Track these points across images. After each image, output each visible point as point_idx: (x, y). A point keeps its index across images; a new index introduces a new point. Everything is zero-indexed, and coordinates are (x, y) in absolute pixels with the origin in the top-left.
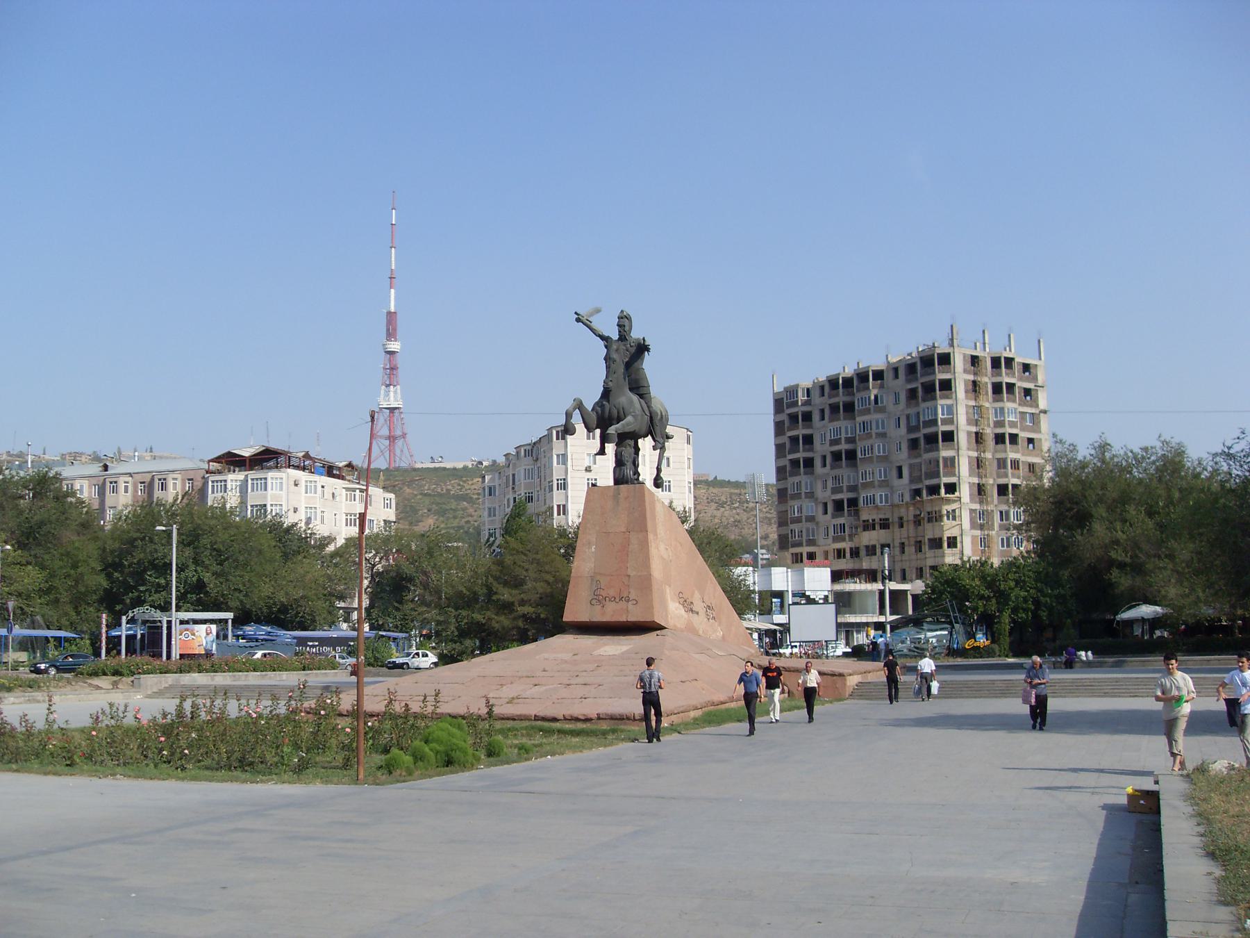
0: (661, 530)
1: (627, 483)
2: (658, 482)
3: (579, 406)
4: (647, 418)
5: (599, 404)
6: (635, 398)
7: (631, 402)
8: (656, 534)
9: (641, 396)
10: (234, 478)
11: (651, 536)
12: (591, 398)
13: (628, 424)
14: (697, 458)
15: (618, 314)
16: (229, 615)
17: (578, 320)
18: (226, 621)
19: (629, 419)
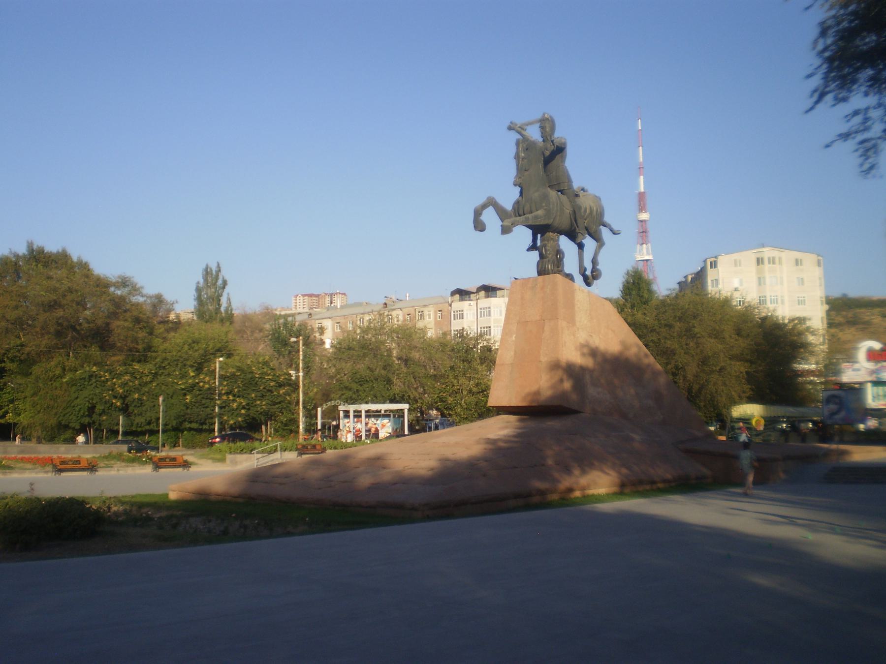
0: (582, 318)
1: (549, 274)
3: (491, 202)
4: (568, 211)
5: (517, 203)
6: (553, 194)
7: (545, 197)
8: (572, 321)
9: (562, 192)
10: (468, 307)
11: (563, 324)
12: (509, 197)
13: (536, 217)
14: (828, 278)
16: (405, 407)
17: (510, 128)
18: (402, 410)
19: (540, 212)
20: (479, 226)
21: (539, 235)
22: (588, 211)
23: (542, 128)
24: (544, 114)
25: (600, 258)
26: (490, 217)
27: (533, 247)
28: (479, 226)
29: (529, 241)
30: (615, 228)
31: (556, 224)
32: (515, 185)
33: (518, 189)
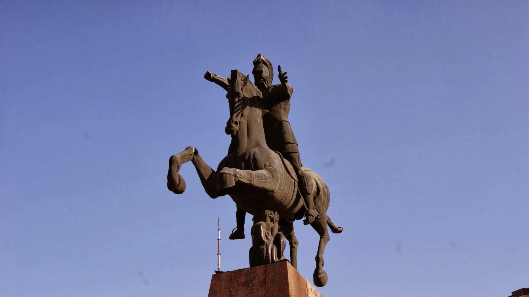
2: (319, 281)
12: (215, 151)
15: (254, 58)
17: (208, 76)
19: (263, 172)
20: (175, 186)
21: (249, 218)
22: (314, 188)
23: (257, 73)
24: (259, 55)
25: (326, 257)
26: (188, 173)
27: (238, 234)
28: (175, 186)
29: (233, 225)
30: (336, 225)
31: (278, 195)
32: (229, 130)
33: (228, 139)
